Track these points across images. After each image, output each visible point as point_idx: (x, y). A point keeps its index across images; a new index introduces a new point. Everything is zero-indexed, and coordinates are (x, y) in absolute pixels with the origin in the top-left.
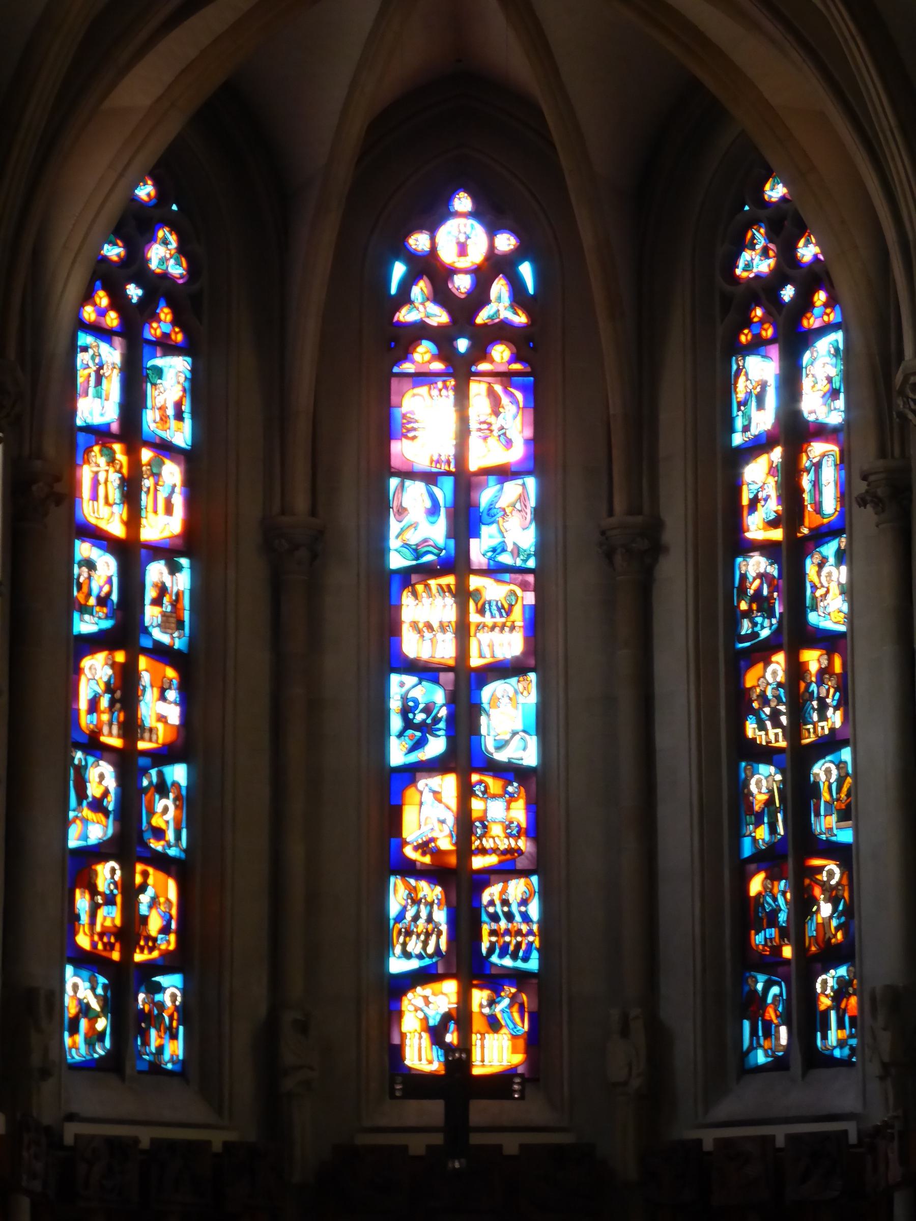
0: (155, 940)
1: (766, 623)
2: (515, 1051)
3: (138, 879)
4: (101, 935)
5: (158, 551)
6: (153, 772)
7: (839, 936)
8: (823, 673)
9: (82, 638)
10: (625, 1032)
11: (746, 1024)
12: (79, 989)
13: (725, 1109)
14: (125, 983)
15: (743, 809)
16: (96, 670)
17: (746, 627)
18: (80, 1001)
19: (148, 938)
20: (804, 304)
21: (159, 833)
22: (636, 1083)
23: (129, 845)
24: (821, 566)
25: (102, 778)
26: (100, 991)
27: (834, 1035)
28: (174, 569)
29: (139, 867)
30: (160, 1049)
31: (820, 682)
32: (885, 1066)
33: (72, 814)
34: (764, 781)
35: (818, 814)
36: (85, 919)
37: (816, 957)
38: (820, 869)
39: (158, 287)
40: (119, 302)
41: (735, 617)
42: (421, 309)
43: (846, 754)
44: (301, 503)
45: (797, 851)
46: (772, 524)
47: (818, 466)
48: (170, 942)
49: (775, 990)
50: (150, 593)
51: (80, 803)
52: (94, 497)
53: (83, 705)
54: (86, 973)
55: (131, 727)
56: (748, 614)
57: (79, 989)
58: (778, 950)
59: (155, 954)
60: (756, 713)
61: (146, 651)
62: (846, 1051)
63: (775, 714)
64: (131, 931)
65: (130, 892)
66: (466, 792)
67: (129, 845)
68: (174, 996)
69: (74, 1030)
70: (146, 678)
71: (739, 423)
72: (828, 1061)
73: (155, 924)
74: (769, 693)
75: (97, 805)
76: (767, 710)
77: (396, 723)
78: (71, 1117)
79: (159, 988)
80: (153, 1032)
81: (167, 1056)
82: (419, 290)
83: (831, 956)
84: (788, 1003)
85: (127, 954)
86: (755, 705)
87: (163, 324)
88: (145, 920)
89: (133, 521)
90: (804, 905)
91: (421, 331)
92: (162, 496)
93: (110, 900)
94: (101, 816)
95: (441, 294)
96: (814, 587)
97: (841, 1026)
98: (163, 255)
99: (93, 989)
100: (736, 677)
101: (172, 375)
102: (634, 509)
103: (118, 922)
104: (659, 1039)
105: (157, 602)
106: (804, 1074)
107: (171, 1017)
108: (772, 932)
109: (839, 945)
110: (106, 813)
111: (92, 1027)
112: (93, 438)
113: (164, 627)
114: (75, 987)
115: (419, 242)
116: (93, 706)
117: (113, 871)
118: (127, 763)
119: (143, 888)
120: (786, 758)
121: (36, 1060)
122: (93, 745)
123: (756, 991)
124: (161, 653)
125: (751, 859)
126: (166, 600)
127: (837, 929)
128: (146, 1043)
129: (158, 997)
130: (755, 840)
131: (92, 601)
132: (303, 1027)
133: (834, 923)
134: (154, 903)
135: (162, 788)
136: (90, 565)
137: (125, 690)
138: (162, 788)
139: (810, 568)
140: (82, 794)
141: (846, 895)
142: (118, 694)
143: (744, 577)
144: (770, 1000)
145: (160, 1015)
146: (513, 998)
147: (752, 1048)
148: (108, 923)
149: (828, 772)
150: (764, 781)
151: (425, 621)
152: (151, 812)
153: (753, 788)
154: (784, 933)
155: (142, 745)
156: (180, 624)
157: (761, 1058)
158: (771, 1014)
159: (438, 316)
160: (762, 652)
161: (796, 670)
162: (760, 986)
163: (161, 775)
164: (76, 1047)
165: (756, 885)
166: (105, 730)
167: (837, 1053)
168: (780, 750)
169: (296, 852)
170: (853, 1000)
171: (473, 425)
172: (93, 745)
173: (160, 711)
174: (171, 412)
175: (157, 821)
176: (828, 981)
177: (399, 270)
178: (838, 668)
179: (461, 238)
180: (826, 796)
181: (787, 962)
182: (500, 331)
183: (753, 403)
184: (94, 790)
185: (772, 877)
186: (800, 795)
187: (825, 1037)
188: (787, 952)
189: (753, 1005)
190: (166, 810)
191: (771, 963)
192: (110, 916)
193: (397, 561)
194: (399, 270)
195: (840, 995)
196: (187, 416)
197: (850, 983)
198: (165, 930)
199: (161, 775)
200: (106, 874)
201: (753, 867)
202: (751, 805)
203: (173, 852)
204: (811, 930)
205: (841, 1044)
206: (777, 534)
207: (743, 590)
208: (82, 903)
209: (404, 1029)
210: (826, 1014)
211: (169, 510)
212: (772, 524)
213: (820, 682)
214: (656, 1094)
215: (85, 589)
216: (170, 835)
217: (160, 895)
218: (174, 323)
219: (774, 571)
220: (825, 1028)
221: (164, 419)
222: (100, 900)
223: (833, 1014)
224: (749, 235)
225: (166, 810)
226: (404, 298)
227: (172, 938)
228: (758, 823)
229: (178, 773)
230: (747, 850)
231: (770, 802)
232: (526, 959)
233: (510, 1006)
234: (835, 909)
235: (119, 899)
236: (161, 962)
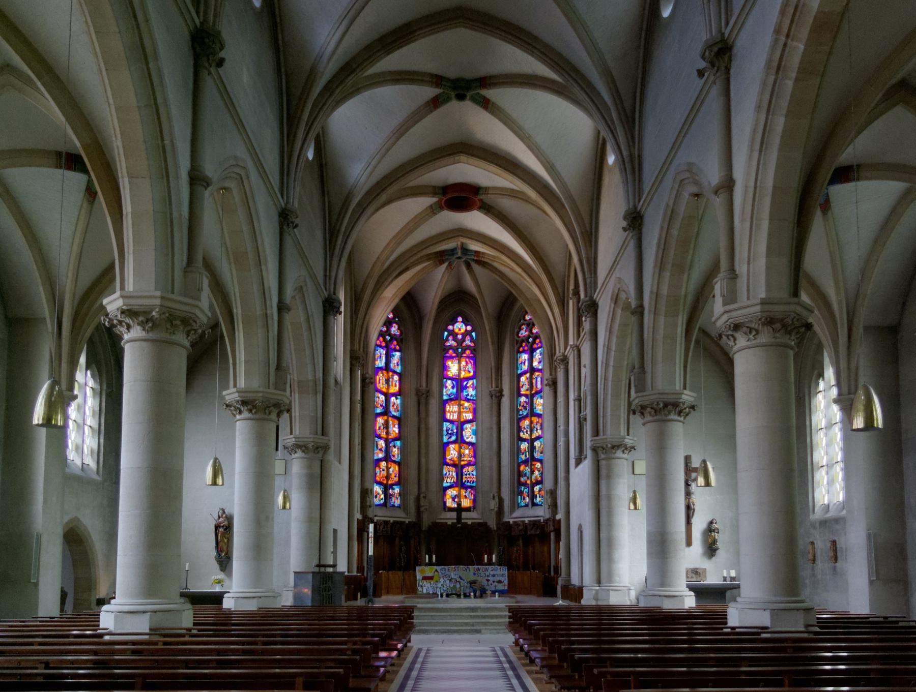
10: (494, 498)
13: (514, 515)
14: (386, 488)
17: (521, 413)
23: (387, 458)
25: (382, 443)
27: (538, 499)
39: (393, 337)
41: (518, 411)
42: (451, 342)
44: (424, 385)
48: (396, 479)
55: (388, 433)
57: (377, 489)
64: (388, 477)
65: (388, 469)
67: (387, 458)
72: (537, 505)
73: (393, 476)
75: (381, 450)
77: (445, 433)
82: (450, 338)
90: (532, 472)
91: (451, 347)
95: (455, 339)
104: (501, 501)
115: (450, 327)
118: (387, 442)
124: (394, 417)
132: (425, 497)
137: (386, 425)
138: (394, 446)
150: (524, 446)
151: (452, 411)
159: (454, 343)
160: (525, 417)
161: (531, 422)
164: (377, 501)
169: (423, 460)
177: (446, 333)
179: (460, 327)
182: (468, 347)
186: (532, 448)
189: (521, 493)
191: (525, 484)
193: (445, 398)
194: (446, 333)
195: (540, 490)
200: (383, 464)
208: (378, 470)
214: (500, 512)
217: (394, 469)
226: (447, 340)
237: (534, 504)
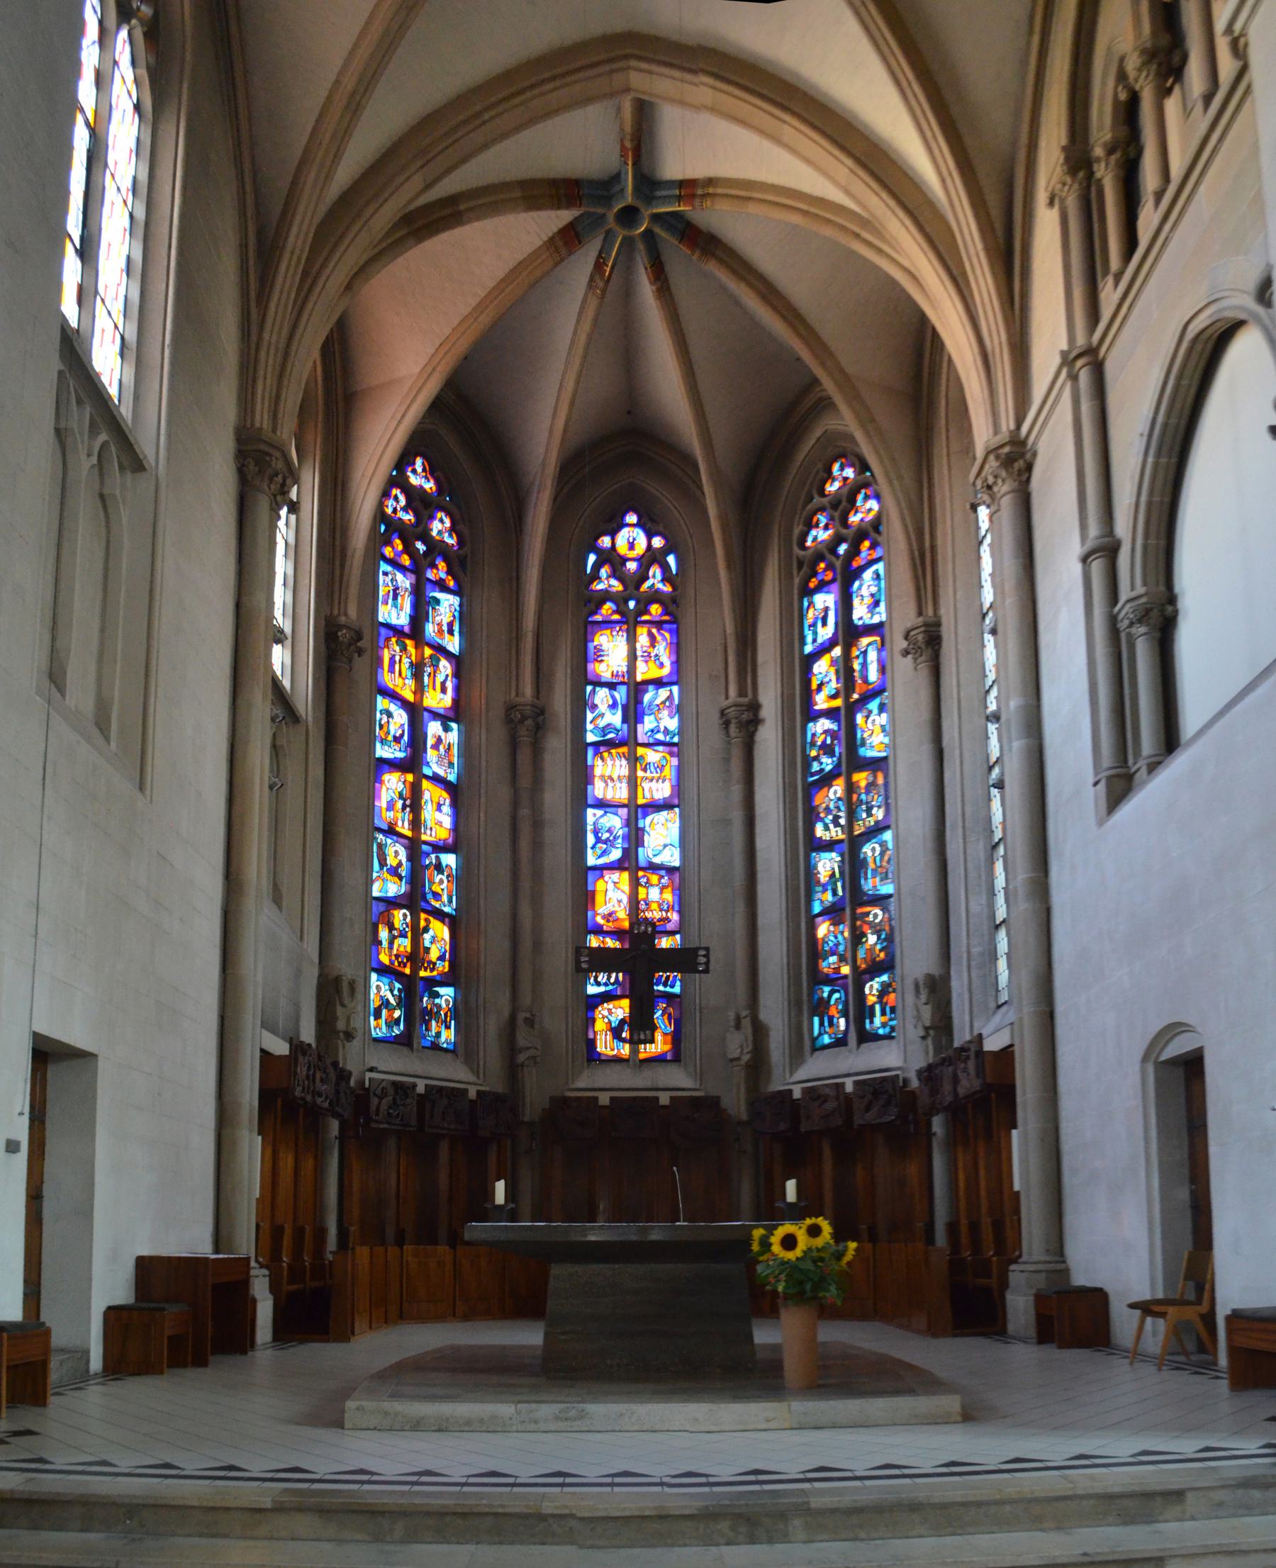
0: (435, 964)
1: (829, 761)
2: (665, 1043)
3: (423, 923)
4: (397, 956)
5: (435, 715)
6: (433, 856)
7: (882, 955)
8: (871, 786)
9: (382, 761)
10: (738, 1026)
11: (816, 1020)
12: (380, 988)
13: (802, 1074)
14: (413, 989)
15: (813, 883)
16: (393, 784)
17: (815, 767)
18: (382, 997)
19: (430, 962)
20: (854, 551)
21: (437, 896)
22: (746, 1058)
23: (415, 899)
24: (867, 717)
25: (397, 853)
26: (396, 992)
27: (878, 1020)
28: (447, 729)
29: (423, 916)
30: (438, 1034)
31: (867, 792)
32: (927, 1029)
33: (375, 875)
34: (827, 864)
35: (866, 879)
36: (385, 944)
37: (865, 972)
38: (868, 914)
39: (436, 548)
40: (409, 549)
41: (807, 761)
43: (888, 836)
44: (528, 691)
45: (853, 902)
46: (833, 697)
47: (865, 653)
48: (443, 967)
49: (836, 995)
50: (430, 741)
51: (381, 868)
52: (391, 670)
53: (383, 803)
54: (386, 980)
55: (416, 824)
56: (816, 758)
57: (380, 988)
58: (837, 970)
59: (435, 973)
60: (821, 820)
61: (427, 777)
62: (888, 1029)
63: (836, 818)
64: (417, 956)
65: (417, 933)
66: (635, 883)
67: (415, 899)
68: (447, 1001)
69: (378, 1015)
70: (427, 796)
71: (809, 639)
72: (876, 1037)
73: (434, 954)
74: (832, 806)
75: (394, 871)
76: (830, 817)
79: (437, 995)
80: (434, 1022)
81: (443, 1039)
83: (876, 968)
84: (846, 1003)
85: (415, 971)
86: (822, 815)
87: (440, 571)
88: (427, 950)
89: (420, 690)
90: (857, 938)
92: (440, 678)
93: (403, 935)
94: (396, 879)
96: (863, 731)
97: (883, 1013)
98: (440, 526)
99: (392, 991)
100: (808, 798)
101: (447, 605)
102: (742, 693)
103: (409, 949)
104: (760, 1032)
105: (436, 747)
106: (858, 1046)
107: (446, 1015)
108: (833, 959)
109: (882, 962)
110: (400, 878)
111: (391, 1016)
112: (391, 633)
113: (439, 763)
114: (378, 987)
116: (391, 806)
117: (405, 915)
118: (414, 846)
119: (426, 929)
120: (845, 846)
121: (341, 1025)
122: (391, 831)
123: (822, 998)
124: (436, 779)
125: (819, 915)
126: (441, 748)
127: (881, 951)
128: (428, 1029)
129: (437, 1001)
130: (822, 902)
131: (390, 738)
132: (530, 1022)
133: (878, 947)
134: (433, 940)
135: (439, 867)
136: (390, 715)
137: (414, 802)
139: (859, 718)
140: (383, 863)
141: (887, 928)
142: (408, 802)
143: (814, 735)
144: (832, 1002)
145: (438, 1012)
146: (664, 1011)
147: (820, 1034)
148: (402, 949)
149: (873, 850)
150: (827, 864)
152: (432, 882)
153: (820, 867)
154: (842, 959)
155: (424, 837)
156: (451, 764)
157: (826, 1040)
158: (833, 1011)
160: (826, 780)
161: (851, 788)
162: (825, 995)
163: (437, 858)
164: (379, 1028)
165: (823, 929)
166: (400, 823)
167: (881, 1032)
168: (841, 841)
170: (892, 996)
171: (639, 653)
172: (391, 831)
173: (438, 820)
174: (445, 628)
175: (436, 888)
176: (872, 988)
178: (880, 780)
180: (872, 866)
181: (846, 977)
183: (819, 624)
184: (391, 861)
185: (835, 923)
186: (854, 866)
187: (872, 1022)
188: (845, 970)
189: (821, 1007)
190: (441, 882)
191: (834, 980)
192: (404, 944)
195: (883, 992)
196: (456, 633)
197: (889, 985)
198: (441, 958)
199: (437, 858)
200: (400, 917)
201: (819, 919)
202: (818, 882)
203: (447, 909)
204: (861, 954)
205: (884, 1025)
206: (838, 702)
207: (813, 744)
208: (384, 934)
209: (597, 1029)
210: (872, 1008)
211: (444, 690)
212: (833, 697)
213: (867, 792)
214: (758, 1065)
215: (385, 729)
216: (445, 898)
217: (438, 936)
218: (448, 573)
219: (834, 727)
220: (872, 1015)
221: (440, 632)
222: (395, 933)
223: (877, 1007)
224: (815, 520)
225: (441, 882)
227: (447, 964)
228: (825, 890)
229: (449, 860)
230: (817, 908)
231: (833, 875)
232: (672, 987)
233: (662, 1015)
234: (879, 938)
235: (409, 935)
236: (438, 978)
237: (866, 1037)
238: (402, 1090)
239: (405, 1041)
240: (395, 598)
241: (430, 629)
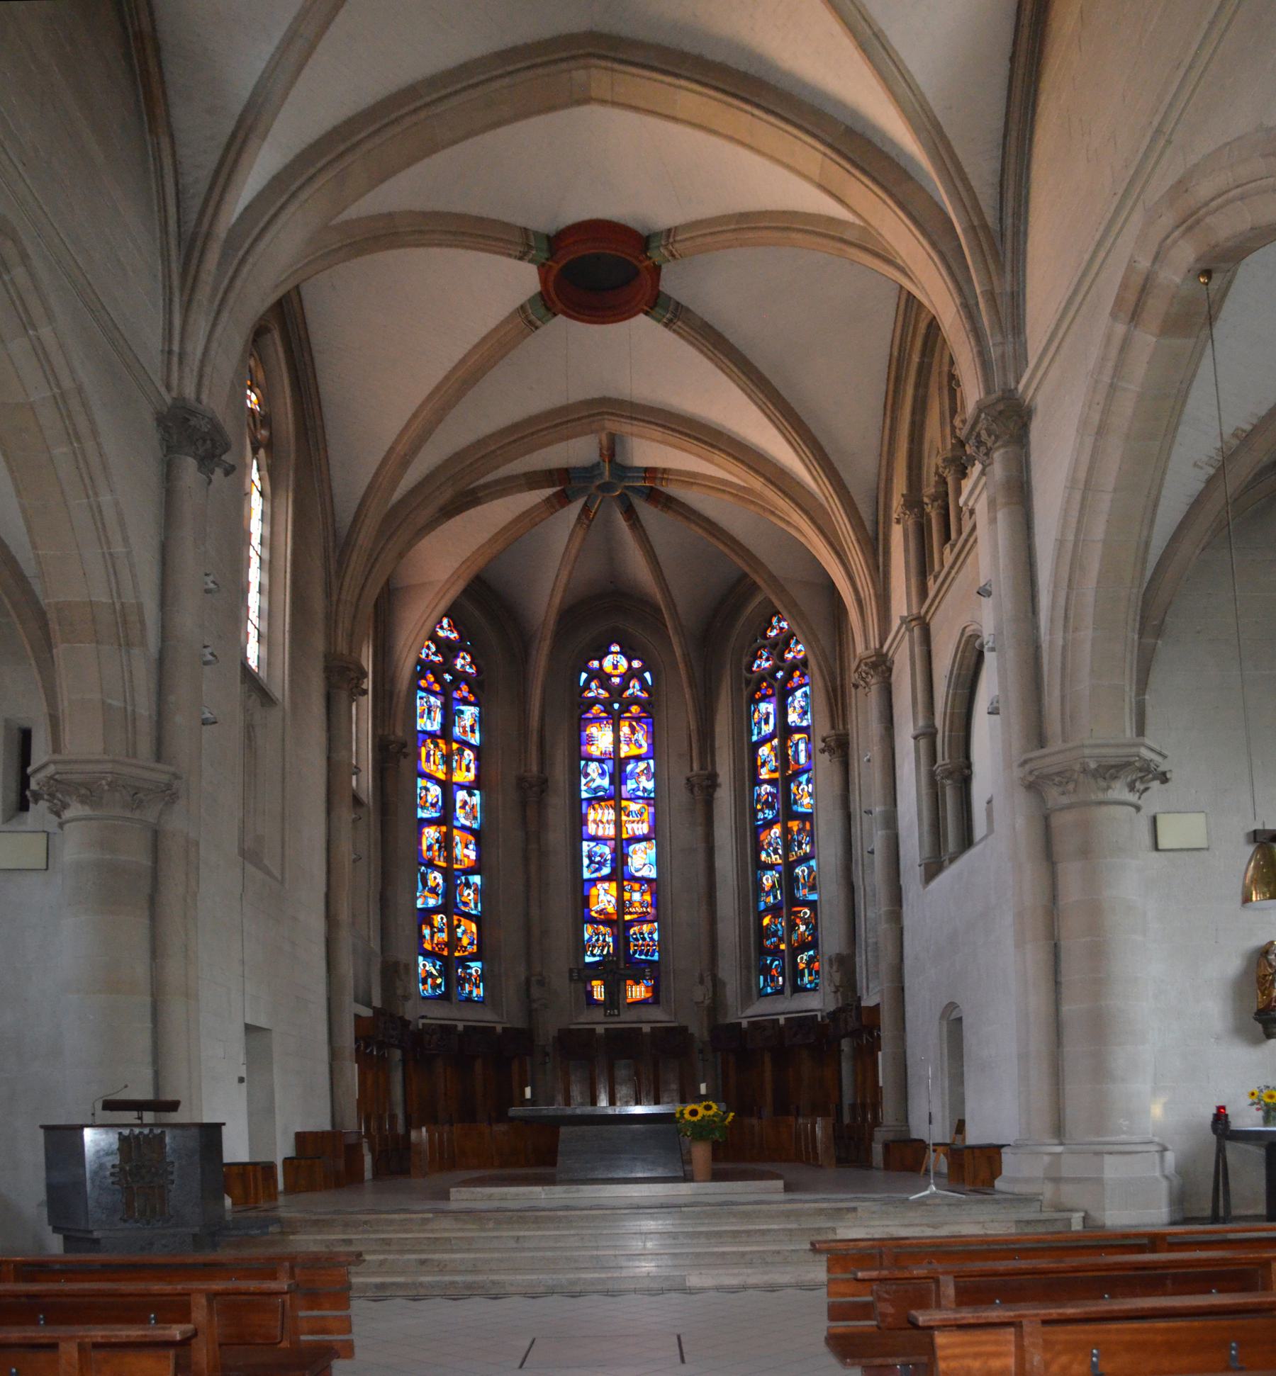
3: (456, 922)
5: (461, 786)
9: (422, 819)
14: (450, 963)
21: (466, 904)
23: (449, 906)
25: (436, 878)
28: (471, 794)
29: (455, 917)
30: (471, 992)
36: (428, 937)
39: (460, 677)
40: (439, 680)
50: (458, 804)
52: (428, 760)
53: (424, 848)
55: (450, 858)
61: (456, 828)
64: (453, 942)
65: (452, 929)
67: (449, 906)
69: (424, 982)
70: (457, 839)
73: (465, 941)
75: (433, 890)
78: (423, 1017)
79: (470, 968)
88: (460, 939)
89: (450, 771)
98: (462, 662)
101: (469, 713)
105: (463, 807)
111: (434, 981)
113: (466, 818)
116: (430, 848)
118: (447, 873)
119: (459, 926)
122: (430, 864)
124: (463, 828)
128: (463, 989)
134: (464, 932)
135: (468, 885)
136: (427, 789)
137: (446, 843)
138: (468, 885)
152: (461, 895)
155: (456, 866)
156: (475, 818)
163: (467, 880)
164: (426, 990)
172: (430, 864)
173: (466, 853)
184: (431, 883)
198: (471, 944)
200: (438, 919)
203: (474, 912)
208: (427, 932)
211: (468, 770)
216: (472, 905)
217: (467, 931)
221: (465, 732)
229: (476, 879)
238: (447, 1030)
239: (446, 997)
240: (429, 712)
241: (457, 731)
